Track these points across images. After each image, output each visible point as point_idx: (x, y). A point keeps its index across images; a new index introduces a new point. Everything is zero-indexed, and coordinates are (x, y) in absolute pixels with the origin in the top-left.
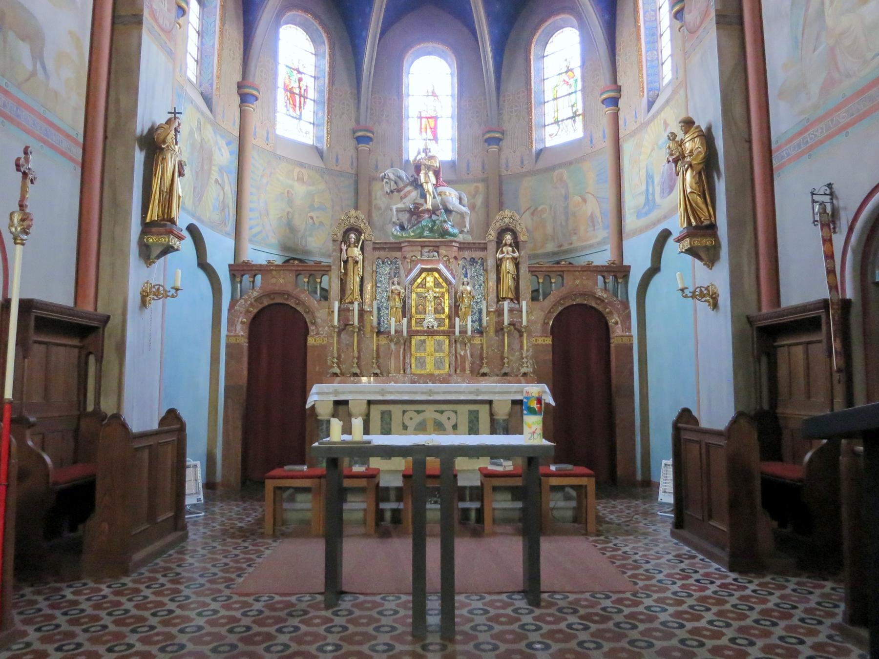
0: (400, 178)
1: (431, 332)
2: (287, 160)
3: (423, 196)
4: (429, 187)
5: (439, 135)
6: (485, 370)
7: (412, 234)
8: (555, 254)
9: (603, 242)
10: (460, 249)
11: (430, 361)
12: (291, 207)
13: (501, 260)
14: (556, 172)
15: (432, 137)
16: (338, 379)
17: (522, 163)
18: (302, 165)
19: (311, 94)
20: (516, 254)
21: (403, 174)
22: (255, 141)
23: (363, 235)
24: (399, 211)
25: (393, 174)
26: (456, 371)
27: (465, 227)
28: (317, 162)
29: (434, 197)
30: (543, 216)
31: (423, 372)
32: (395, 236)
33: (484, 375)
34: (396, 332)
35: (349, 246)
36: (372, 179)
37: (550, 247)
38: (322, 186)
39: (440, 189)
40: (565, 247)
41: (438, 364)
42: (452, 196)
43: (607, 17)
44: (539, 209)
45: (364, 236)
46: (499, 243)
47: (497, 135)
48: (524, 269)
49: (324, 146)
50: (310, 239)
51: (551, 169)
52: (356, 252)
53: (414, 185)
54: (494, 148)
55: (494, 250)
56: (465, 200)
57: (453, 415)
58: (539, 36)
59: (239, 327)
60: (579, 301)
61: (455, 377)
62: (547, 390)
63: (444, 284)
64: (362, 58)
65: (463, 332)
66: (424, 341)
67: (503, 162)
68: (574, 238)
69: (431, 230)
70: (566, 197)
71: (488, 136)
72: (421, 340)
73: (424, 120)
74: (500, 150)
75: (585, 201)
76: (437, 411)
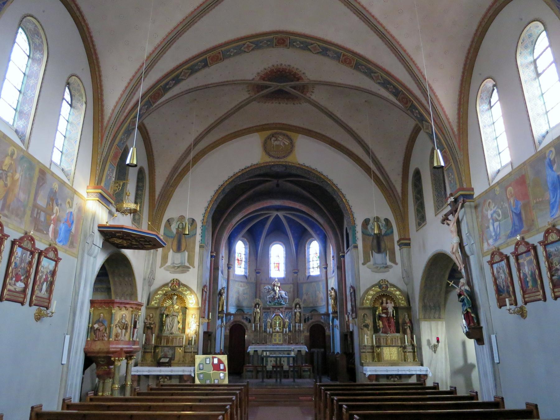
0: (269, 288)
1: (278, 332)
3: (276, 293)
4: (277, 291)
5: (280, 269)
6: (292, 342)
9: (324, 306)
11: (277, 340)
13: (296, 312)
15: (278, 269)
16: (254, 344)
18: (241, 282)
19: (244, 260)
22: (231, 278)
28: (245, 280)
31: (276, 343)
32: (268, 305)
33: (292, 343)
35: (256, 308)
36: (261, 283)
37: (311, 305)
38: (247, 287)
39: (280, 292)
40: (315, 305)
41: (280, 341)
42: (283, 293)
43: (324, 245)
46: (296, 308)
48: (302, 315)
49: (247, 275)
51: (311, 282)
52: (258, 310)
54: (296, 275)
56: (287, 295)
59: (227, 330)
62: (306, 347)
64: (258, 249)
65: (286, 332)
66: (276, 334)
69: (278, 303)
70: (316, 291)
71: (294, 271)
73: (275, 264)
75: (320, 293)
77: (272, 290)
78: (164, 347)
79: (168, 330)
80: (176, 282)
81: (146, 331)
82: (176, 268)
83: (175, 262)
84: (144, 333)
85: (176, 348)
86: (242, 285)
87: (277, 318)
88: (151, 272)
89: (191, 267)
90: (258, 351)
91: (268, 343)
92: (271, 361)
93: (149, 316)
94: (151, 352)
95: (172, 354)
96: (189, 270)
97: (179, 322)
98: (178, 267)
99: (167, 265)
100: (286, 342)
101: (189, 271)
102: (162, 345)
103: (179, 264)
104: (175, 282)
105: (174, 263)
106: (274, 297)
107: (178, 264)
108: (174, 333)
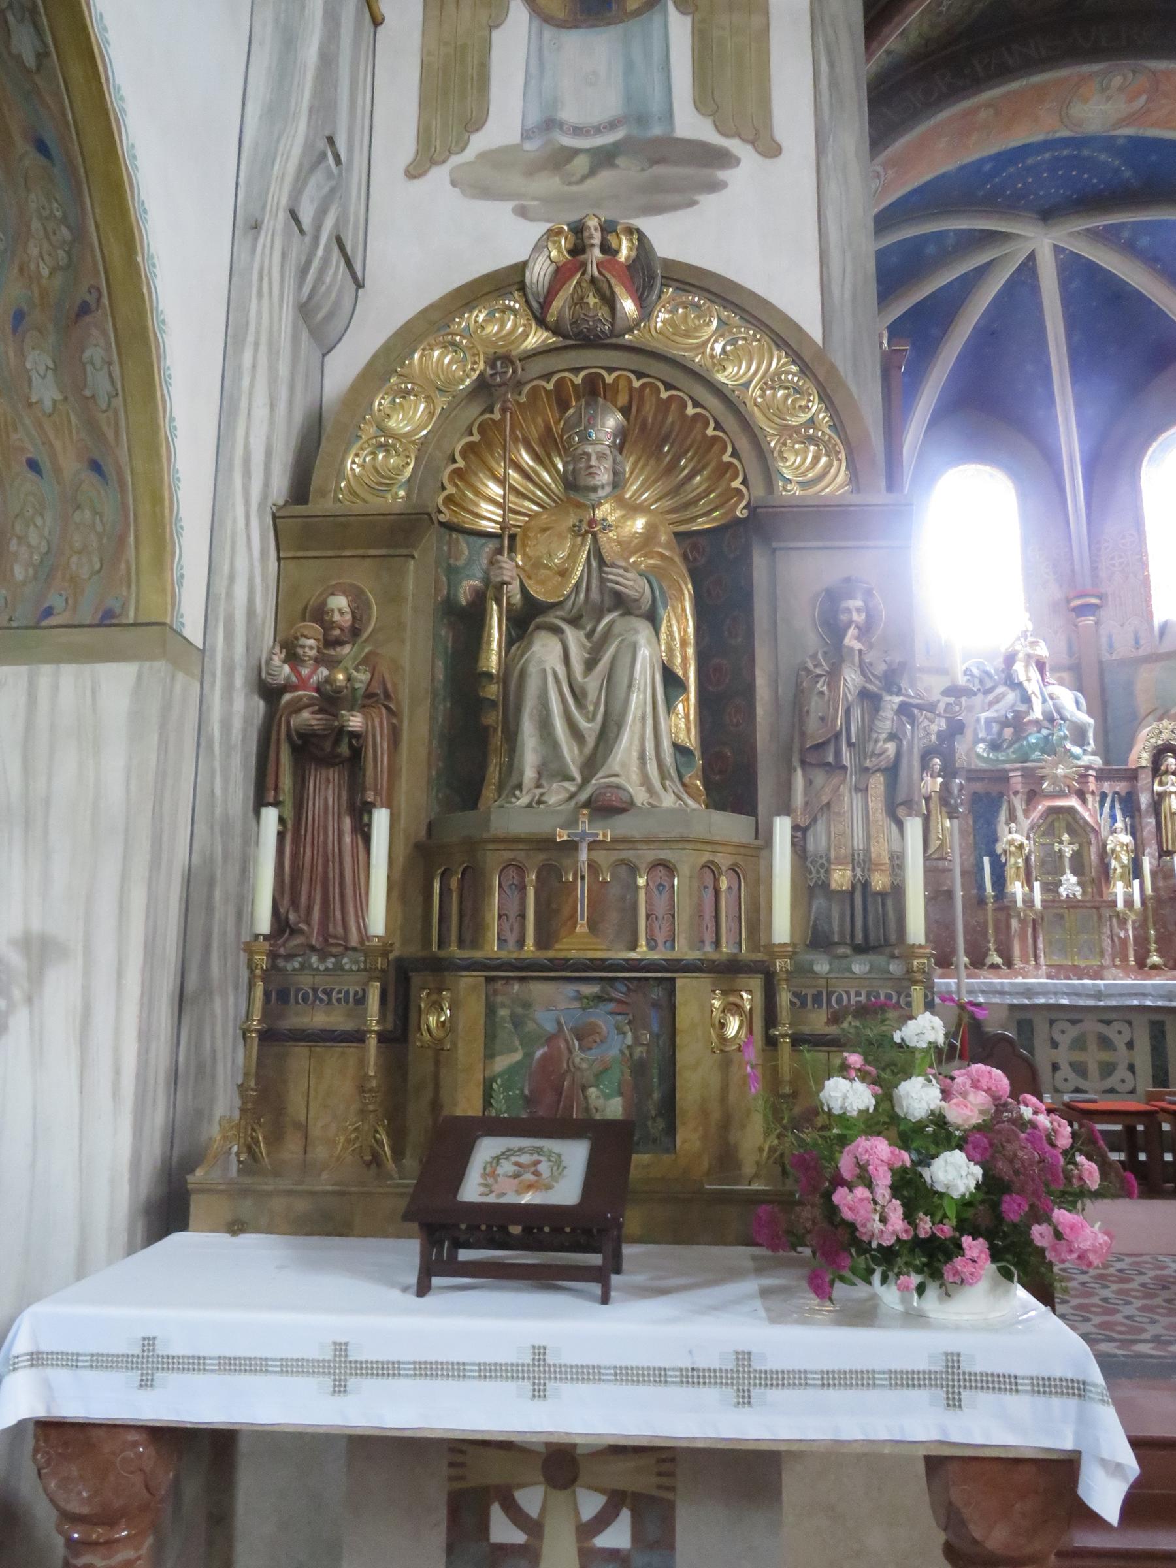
3: (1026, 699)
6: (1155, 959)
10: (1098, 779)
17: (1137, 641)
24: (988, 722)
25: (978, 668)
26: (1113, 961)
27: (1089, 744)
29: (1044, 701)
32: (986, 760)
33: (1154, 967)
34: (1024, 901)
47: (1095, 601)
55: (1150, 780)
57: (1125, 1028)
58: (1154, 452)
61: (1114, 970)
66: (1062, 917)
67: (1104, 640)
74: (1097, 623)
76: (1101, 1021)
77: (1005, 684)
78: (526, 970)
79: (552, 770)
80: (606, 248)
81: (286, 781)
82: (581, 164)
83: (569, 115)
84: (260, 802)
85: (683, 983)
88: (313, 162)
89: (734, 145)
91: (1018, 964)
92: (1055, 1067)
93: (320, 614)
94: (357, 1037)
95: (639, 1069)
96: (723, 175)
97: (672, 682)
98: (604, 158)
99: (480, 142)
100: (1125, 959)
101: (715, 186)
102: (492, 948)
103: (612, 125)
104: (597, 252)
105: (550, 124)
106: (1019, 716)
107: (598, 130)
108: (641, 797)
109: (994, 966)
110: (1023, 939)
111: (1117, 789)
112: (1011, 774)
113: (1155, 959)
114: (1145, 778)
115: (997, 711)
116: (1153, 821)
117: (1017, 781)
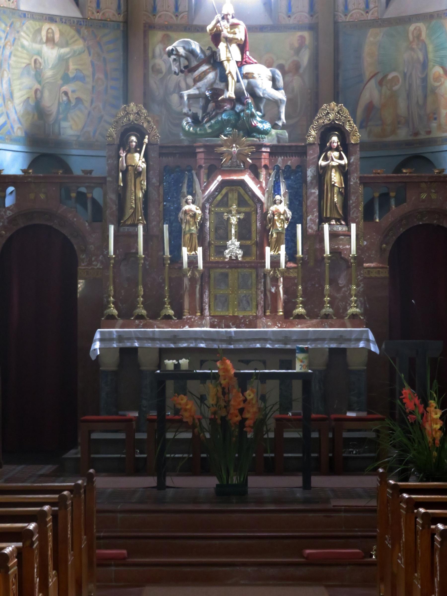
0: (192, 52)
2: (34, 16)
3: (224, 78)
6: (300, 310)
7: (209, 131)
8: (409, 144)
12: (39, 82)
14: (412, 27)
17: (367, 6)
18: (51, 19)
20: (345, 161)
21: (196, 46)
23: (147, 136)
25: (184, 48)
26: (265, 312)
27: (280, 119)
30: (396, 88)
32: (187, 133)
33: (299, 317)
35: (128, 152)
38: (79, 45)
39: (247, 69)
40: (423, 136)
44: (390, 77)
45: (148, 139)
48: (354, 180)
50: (64, 124)
53: (212, 61)
56: (281, 83)
60: (426, 220)
61: (264, 320)
63: (251, 202)
65: (275, 262)
68: (434, 125)
70: (425, 65)
72: (222, 274)
86: (57, 36)
87: (233, 196)
90: (140, 352)
91: (186, 316)
100: (275, 310)
109: (168, 317)
110: (192, 295)
111: (289, 163)
112: (198, 150)
113: (300, 310)
114: (312, 153)
115: (198, 88)
116: (316, 191)
117: (201, 158)
